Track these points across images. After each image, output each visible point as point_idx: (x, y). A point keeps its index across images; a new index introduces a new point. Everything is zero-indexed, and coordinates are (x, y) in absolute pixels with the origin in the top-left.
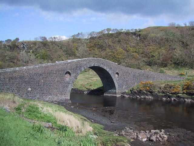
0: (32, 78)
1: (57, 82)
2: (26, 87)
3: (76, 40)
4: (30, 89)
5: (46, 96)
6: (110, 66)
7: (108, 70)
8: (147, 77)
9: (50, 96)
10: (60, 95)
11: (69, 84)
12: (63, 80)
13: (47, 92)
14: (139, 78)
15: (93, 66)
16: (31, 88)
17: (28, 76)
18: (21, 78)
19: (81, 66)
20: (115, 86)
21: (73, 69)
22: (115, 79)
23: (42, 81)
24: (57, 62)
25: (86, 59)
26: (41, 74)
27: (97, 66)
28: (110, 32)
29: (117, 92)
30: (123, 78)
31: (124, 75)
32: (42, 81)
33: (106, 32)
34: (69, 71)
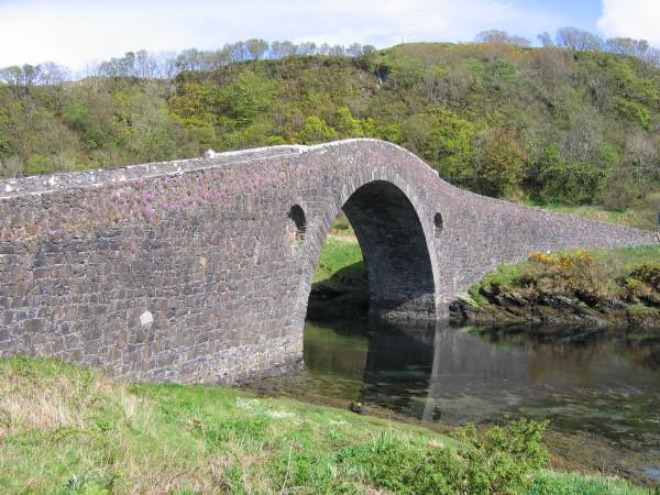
2: (128, 305)
3: (120, 81)
6: (423, 187)
7: (414, 200)
8: (533, 232)
11: (300, 272)
13: (219, 326)
14: (504, 237)
16: (152, 309)
18: (105, 247)
20: (429, 274)
24: (212, 153)
26: (195, 222)
28: (265, 56)
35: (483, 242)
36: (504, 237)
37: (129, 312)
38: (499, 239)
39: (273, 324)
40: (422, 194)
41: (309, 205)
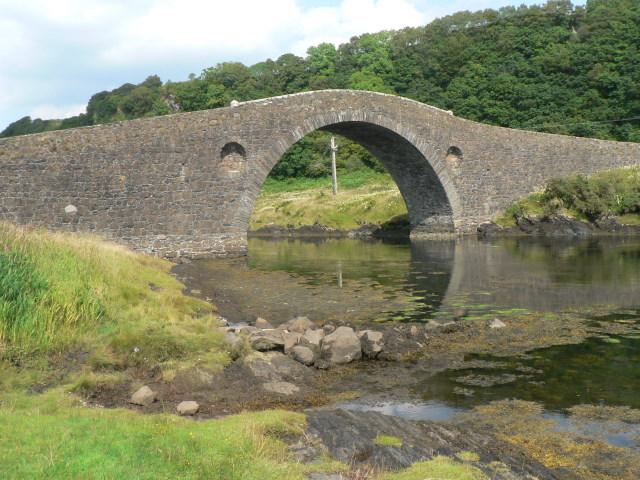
2: (54, 200)
4: (70, 209)
5: (144, 234)
6: (417, 121)
7: (411, 137)
9: (159, 237)
10: (204, 232)
13: (144, 219)
14: (547, 167)
15: (343, 123)
19: (288, 123)
20: (445, 199)
21: (257, 133)
22: (445, 172)
23: (123, 178)
25: (309, 95)
26: (114, 154)
27: (361, 120)
29: (457, 223)
30: (479, 167)
31: (483, 158)
32: (123, 178)
34: (239, 141)
35: (522, 171)
36: (547, 167)
37: (55, 205)
38: (543, 168)
39: (210, 224)
40: (423, 131)
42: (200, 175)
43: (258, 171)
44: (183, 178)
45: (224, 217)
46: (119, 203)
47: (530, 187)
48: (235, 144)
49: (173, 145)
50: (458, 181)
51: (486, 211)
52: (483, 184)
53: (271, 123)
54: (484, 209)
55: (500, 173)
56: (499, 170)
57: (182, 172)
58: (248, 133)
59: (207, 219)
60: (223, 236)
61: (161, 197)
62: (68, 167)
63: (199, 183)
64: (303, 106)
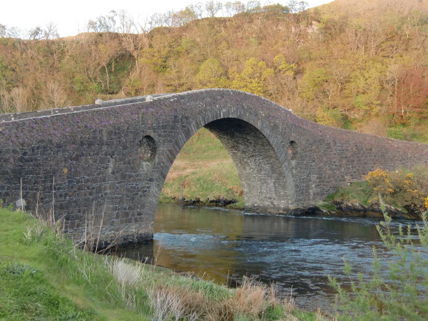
0: (31, 161)
1: (113, 173)
10: (122, 222)
12: (132, 168)
17: (14, 152)
19: (187, 118)
21: (164, 127)
26: (59, 146)
33: (206, 14)
39: (127, 214)
41: (160, 136)
42: (122, 166)
43: (164, 163)
44: (110, 170)
45: (138, 208)
46: (61, 196)
47: (343, 177)
48: (148, 137)
49: (105, 138)
50: (294, 171)
51: (311, 197)
52: (310, 173)
53: (175, 117)
54: (309, 194)
55: (322, 164)
56: (321, 162)
57: (111, 165)
58: (158, 127)
59: (125, 209)
60: (137, 225)
61: (93, 188)
62: (21, 159)
63: (122, 174)
64: (197, 103)
